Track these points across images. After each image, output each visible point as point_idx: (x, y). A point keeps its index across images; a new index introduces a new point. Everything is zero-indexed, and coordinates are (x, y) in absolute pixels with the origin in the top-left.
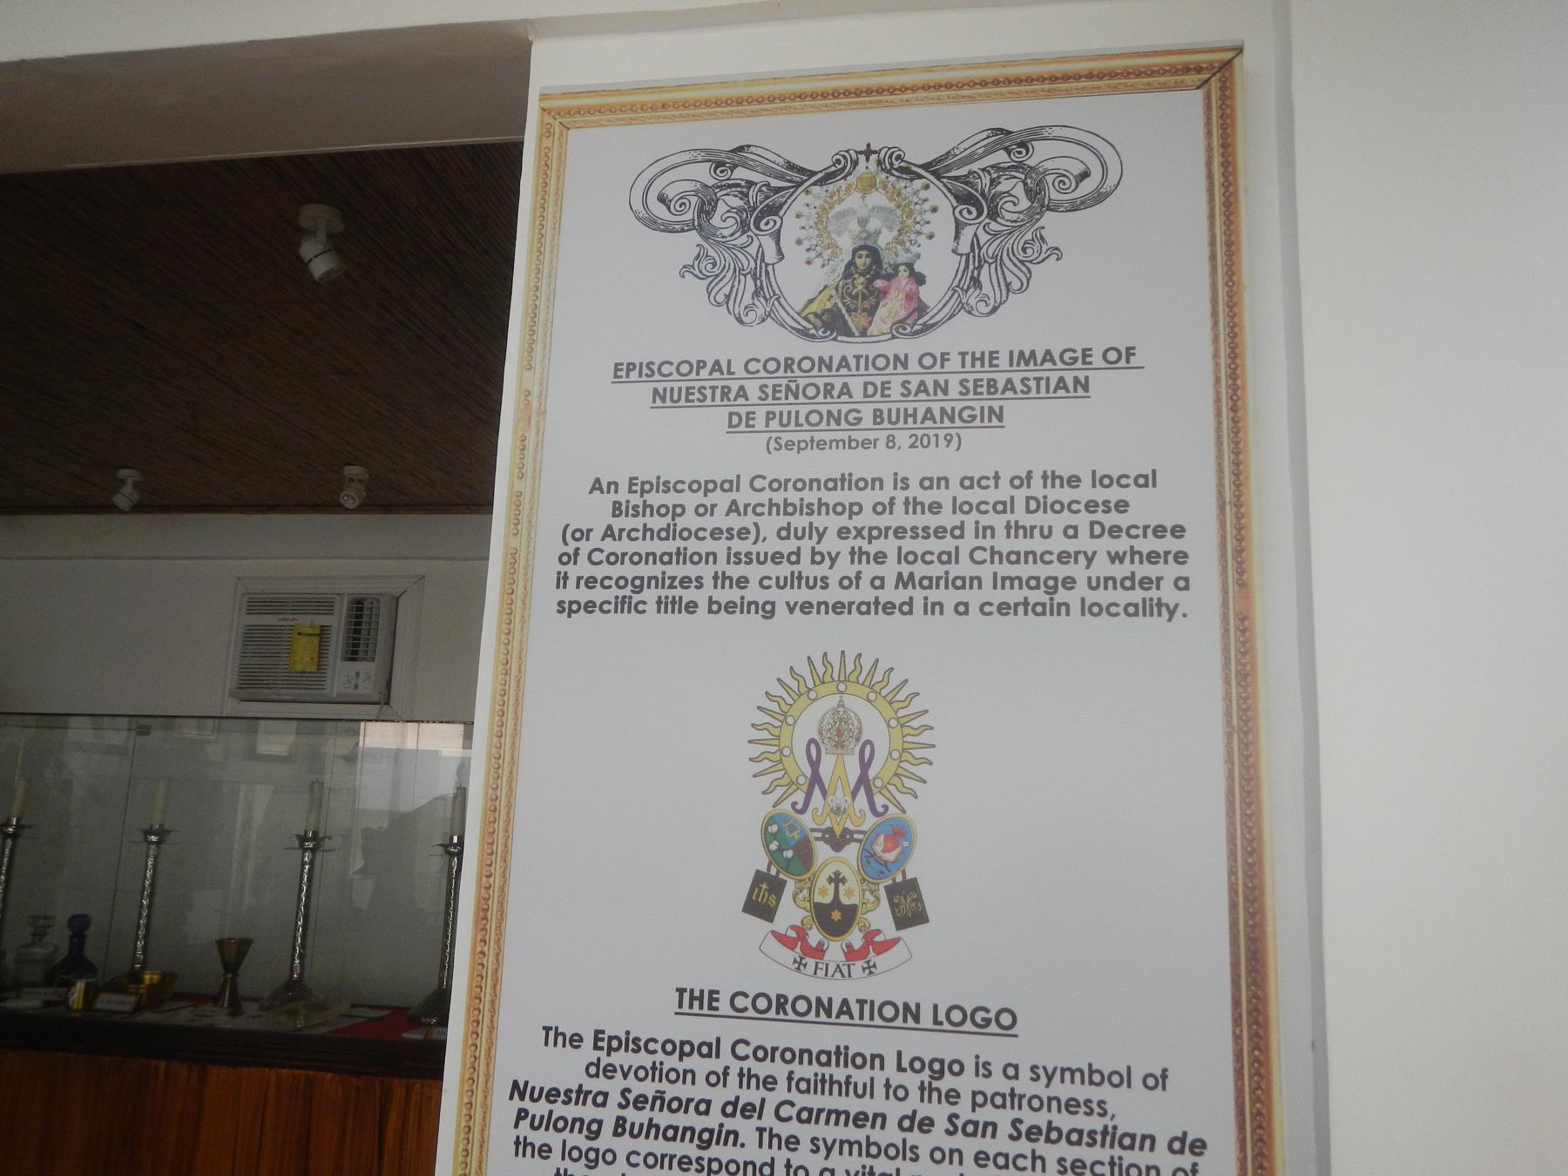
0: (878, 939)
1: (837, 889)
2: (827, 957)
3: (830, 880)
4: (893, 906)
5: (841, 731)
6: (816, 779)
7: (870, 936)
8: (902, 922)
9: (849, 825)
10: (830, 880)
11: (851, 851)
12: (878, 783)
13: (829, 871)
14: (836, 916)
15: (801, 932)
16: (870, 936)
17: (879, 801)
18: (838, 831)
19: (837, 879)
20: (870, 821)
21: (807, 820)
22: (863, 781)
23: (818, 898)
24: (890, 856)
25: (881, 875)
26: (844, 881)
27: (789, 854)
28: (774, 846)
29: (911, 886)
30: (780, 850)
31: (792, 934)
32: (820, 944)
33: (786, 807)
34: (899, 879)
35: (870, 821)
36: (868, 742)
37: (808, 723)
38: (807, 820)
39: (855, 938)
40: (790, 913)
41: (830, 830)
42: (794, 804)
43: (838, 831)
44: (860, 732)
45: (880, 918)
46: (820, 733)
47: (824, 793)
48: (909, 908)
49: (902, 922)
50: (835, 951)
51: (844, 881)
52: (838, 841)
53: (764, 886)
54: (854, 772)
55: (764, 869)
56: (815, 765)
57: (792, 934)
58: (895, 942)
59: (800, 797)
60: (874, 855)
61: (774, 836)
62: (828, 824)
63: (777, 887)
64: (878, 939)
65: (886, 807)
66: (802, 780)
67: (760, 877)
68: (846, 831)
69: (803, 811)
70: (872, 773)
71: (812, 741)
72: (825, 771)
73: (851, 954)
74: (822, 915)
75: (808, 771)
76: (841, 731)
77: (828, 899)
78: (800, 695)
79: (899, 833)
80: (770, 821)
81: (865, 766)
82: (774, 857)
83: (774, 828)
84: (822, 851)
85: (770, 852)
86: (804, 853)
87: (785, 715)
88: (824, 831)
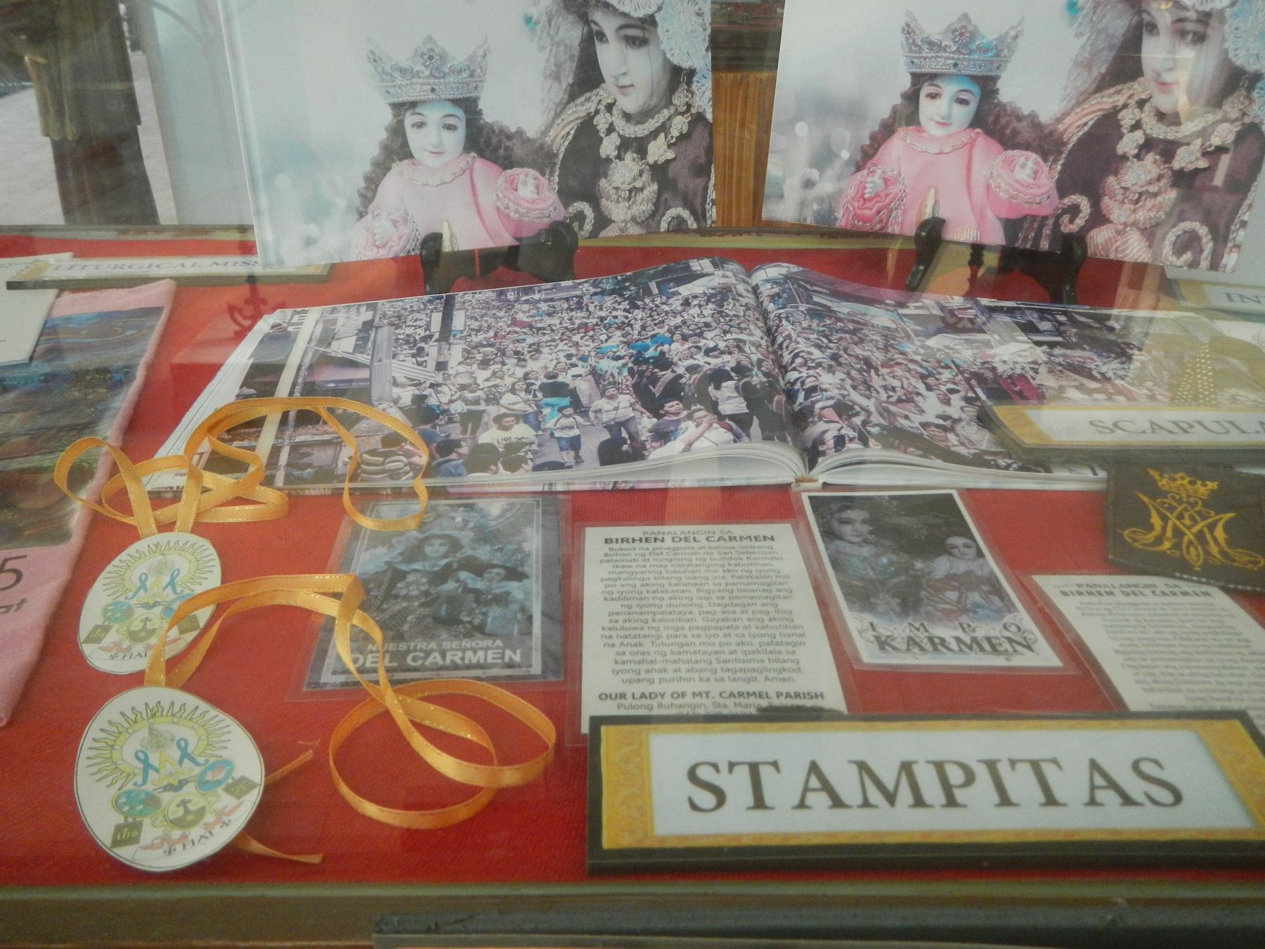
9: (182, 777)
17: (201, 760)
20: (197, 770)
22: (185, 755)
24: (220, 776)
27: (141, 807)
30: (132, 808)
35: (197, 770)
42: (135, 784)
47: (157, 770)
54: (175, 753)
59: (139, 779)
61: (125, 804)
62: (165, 783)
69: (145, 781)
76: (157, 739)
83: (123, 800)
85: (123, 813)
86: (152, 802)
87: (112, 746)
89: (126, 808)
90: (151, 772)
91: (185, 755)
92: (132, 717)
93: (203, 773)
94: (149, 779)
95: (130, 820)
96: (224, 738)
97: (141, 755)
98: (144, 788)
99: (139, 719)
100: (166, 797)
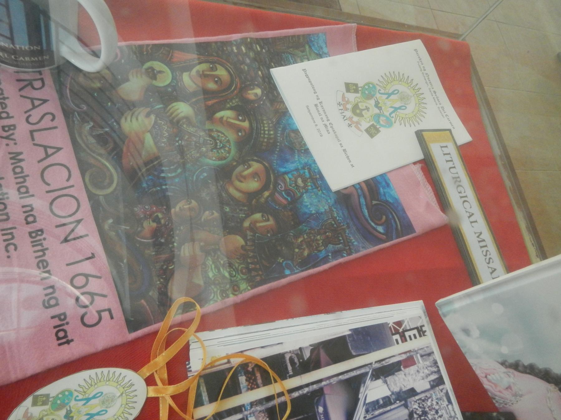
0: (359, 126)
1: (364, 110)
2: (345, 112)
3: (366, 107)
4: (370, 127)
5: (404, 98)
6: (389, 95)
7: (358, 123)
8: (367, 131)
9: (383, 108)
10: (366, 107)
11: (377, 111)
12: (398, 113)
13: (368, 106)
14: (358, 111)
15: (348, 102)
16: (358, 123)
17: (393, 115)
18: (380, 105)
19: (367, 109)
20: (387, 114)
21: (378, 95)
22: (396, 109)
23: (359, 104)
24: (381, 122)
25: (376, 122)
26: (368, 111)
27: (367, 92)
28: (366, 87)
29: (378, 131)
30: (366, 89)
31: (346, 99)
32: (348, 109)
33: (378, 88)
34: (378, 127)
35: (387, 114)
36: (406, 108)
37: (402, 88)
38: (378, 95)
39: (355, 119)
40: (352, 97)
41: (379, 103)
42: (380, 90)
43: (380, 105)
44: (407, 104)
45: (365, 125)
46: (402, 92)
47: (387, 98)
48: (372, 131)
49: (367, 131)
50: (349, 114)
51: (368, 111)
52: (377, 105)
53: (355, 87)
54: (397, 105)
55: (359, 86)
56: (393, 93)
57: (346, 99)
58: (361, 131)
59: (382, 91)
60: (379, 117)
61: (369, 87)
63: (356, 91)
64: (359, 126)
65: (393, 117)
66: (387, 91)
67: (356, 85)
68: (381, 107)
69: (380, 93)
70: (399, 110)
71: (399, 91)
72: (393, 97)
73: (351, 119)
74: (355, 108)
75: (390, 92)
76: (404, 98)
77: (361, 107)
78: (408, 84)
79: (389, 124)
80: (372, 84)
81: (400, 108)
82: (363, 87)
83: (371, 86)
84: (372, 102)
85: (364, 86)
86: (369, 97)
87: (401, 81)
88: (378, 101)
89: (366, 87)
90: (386, 96)
91: (396, 109)
92: (417, 88)
93: (384, 116)
94: (383, 96)
95: (360, 89)
96: (407, 124)
97: (396, 92)
98: (378, 93)
99: (415, 91)
100: (372, 102)
